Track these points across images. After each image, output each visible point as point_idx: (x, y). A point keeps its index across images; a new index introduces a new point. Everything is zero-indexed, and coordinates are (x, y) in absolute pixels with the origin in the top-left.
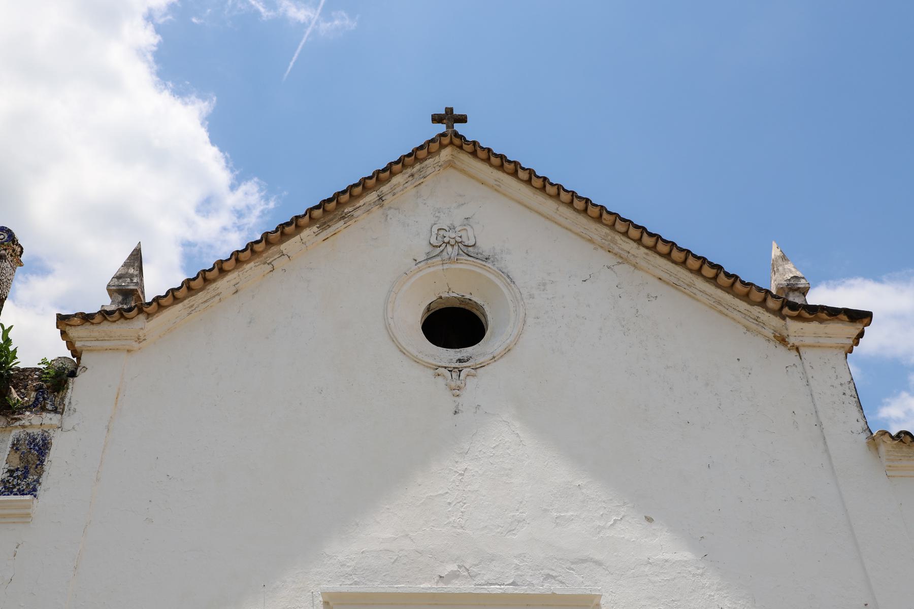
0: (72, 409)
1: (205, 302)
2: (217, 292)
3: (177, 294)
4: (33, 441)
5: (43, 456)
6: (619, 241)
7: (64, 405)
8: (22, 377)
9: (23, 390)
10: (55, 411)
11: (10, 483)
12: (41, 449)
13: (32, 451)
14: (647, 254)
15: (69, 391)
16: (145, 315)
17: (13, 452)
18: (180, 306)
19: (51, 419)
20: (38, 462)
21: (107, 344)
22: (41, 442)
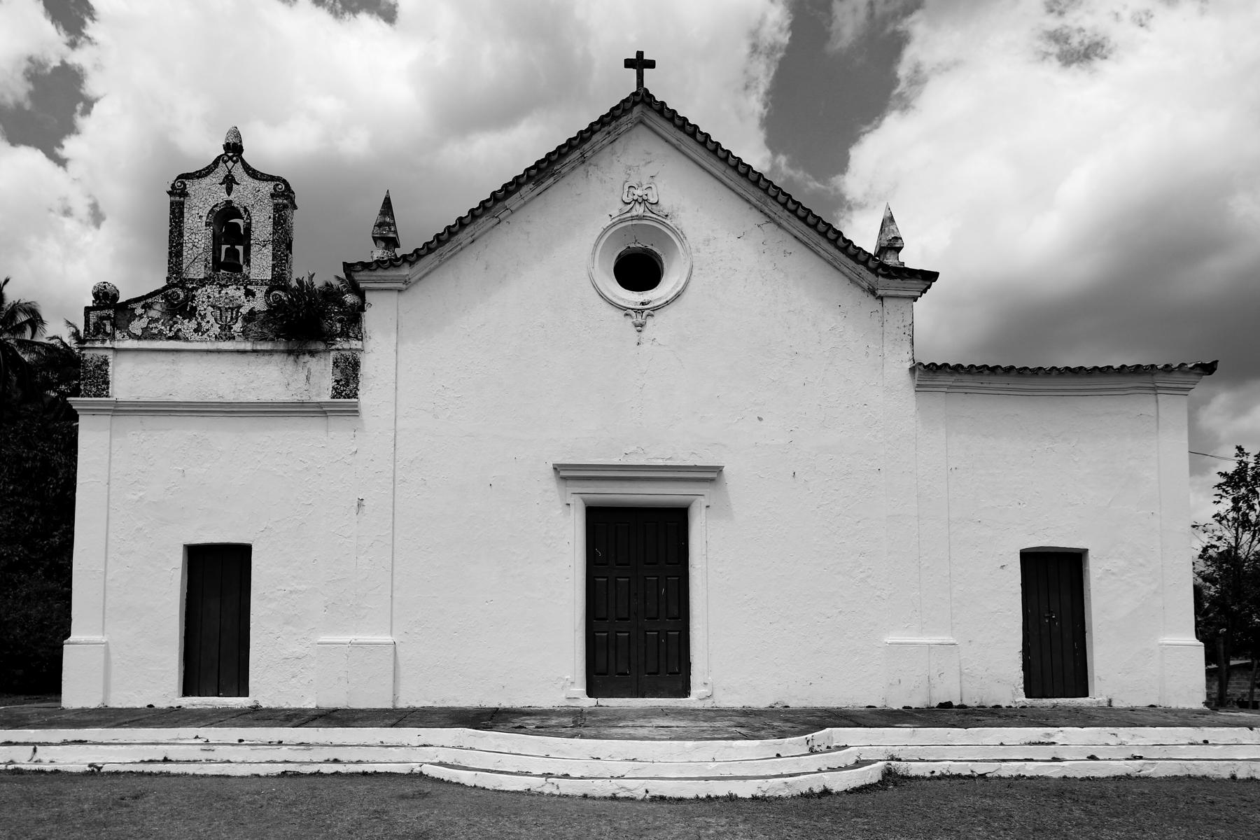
1: (451, 250)
2: (459, 242)
3: (431, 246)
6: (770, 204)
10: (356, 338)
14: (789, 216)
18: (432, 256)
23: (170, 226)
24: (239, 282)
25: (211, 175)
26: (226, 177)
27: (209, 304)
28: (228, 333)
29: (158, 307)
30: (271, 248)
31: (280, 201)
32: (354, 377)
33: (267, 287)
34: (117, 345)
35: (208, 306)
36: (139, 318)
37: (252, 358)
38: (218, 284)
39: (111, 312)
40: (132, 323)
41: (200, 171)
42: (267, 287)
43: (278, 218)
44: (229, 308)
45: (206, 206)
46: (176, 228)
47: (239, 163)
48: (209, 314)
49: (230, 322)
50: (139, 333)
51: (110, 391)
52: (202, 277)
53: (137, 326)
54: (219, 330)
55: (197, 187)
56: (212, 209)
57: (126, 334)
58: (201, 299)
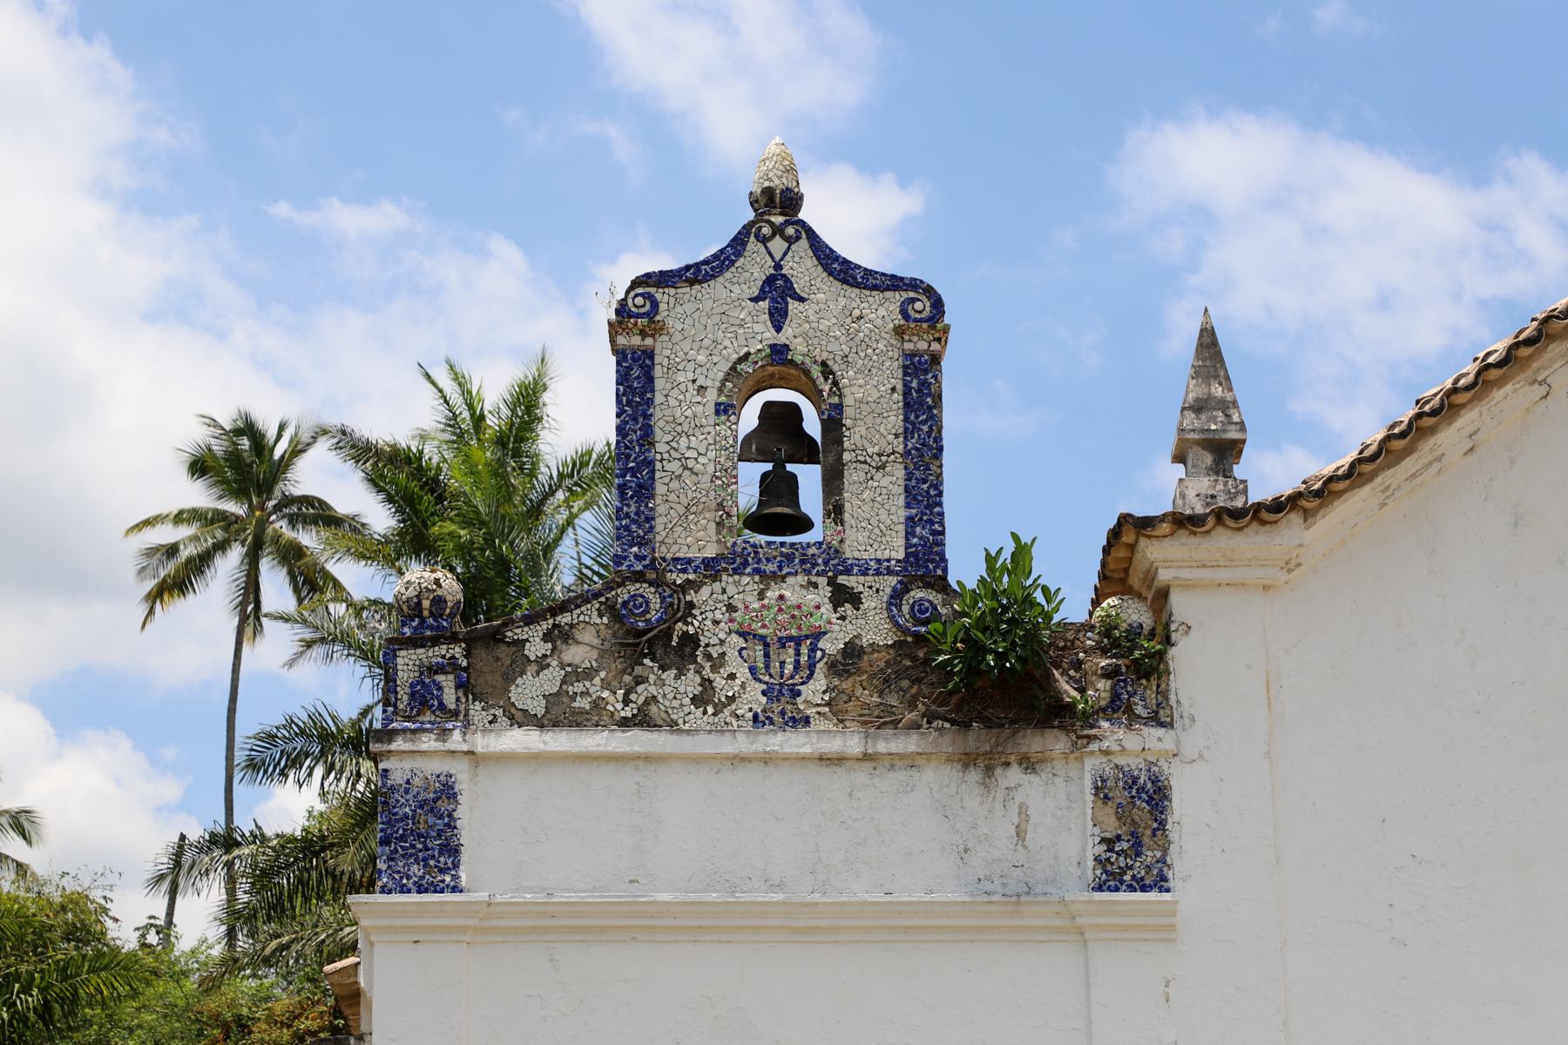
0: (1185, 715)
4: (1134, 782)
5: (1161, 813)
7: (1172, 707)
8: (1062, 644)
9: (1072, 673)
11: (1112, 864)
12: (1154, 799)
13: (1138, 803)
15: (1172, 676)
16: (1301, 513)
17: (1100, 803)
20: (1155, 825)
21: (1224, 575)
22: (1149, 785)
23: (618, 416)
24: (815, 565)
25: (728, 275)
26: (770, 280)
27: (734, 626)
28: (789, 707)
29: (587, 636)
30: (900, 473)
31: (922, 345)
32: (1154, 831)
33: (893, 580)
36: (534, 668)
37: (859, 775)
38: (757, 571)
39: (458, 651)
40: (519, 681)
41: (697, 265)
42: (893, 580)
44: (791, 638)
45: (715, 359)
46: (635, 420)
47: (804, 243)
48: (732, 654)
49: (792, 677)
50: (538, 708)
51: (463, 876)
52: (710, 552)
53: (530, 691)
54: (764, 700)
55: (689, 307)
56: (733, 368)
57: (499, 712)
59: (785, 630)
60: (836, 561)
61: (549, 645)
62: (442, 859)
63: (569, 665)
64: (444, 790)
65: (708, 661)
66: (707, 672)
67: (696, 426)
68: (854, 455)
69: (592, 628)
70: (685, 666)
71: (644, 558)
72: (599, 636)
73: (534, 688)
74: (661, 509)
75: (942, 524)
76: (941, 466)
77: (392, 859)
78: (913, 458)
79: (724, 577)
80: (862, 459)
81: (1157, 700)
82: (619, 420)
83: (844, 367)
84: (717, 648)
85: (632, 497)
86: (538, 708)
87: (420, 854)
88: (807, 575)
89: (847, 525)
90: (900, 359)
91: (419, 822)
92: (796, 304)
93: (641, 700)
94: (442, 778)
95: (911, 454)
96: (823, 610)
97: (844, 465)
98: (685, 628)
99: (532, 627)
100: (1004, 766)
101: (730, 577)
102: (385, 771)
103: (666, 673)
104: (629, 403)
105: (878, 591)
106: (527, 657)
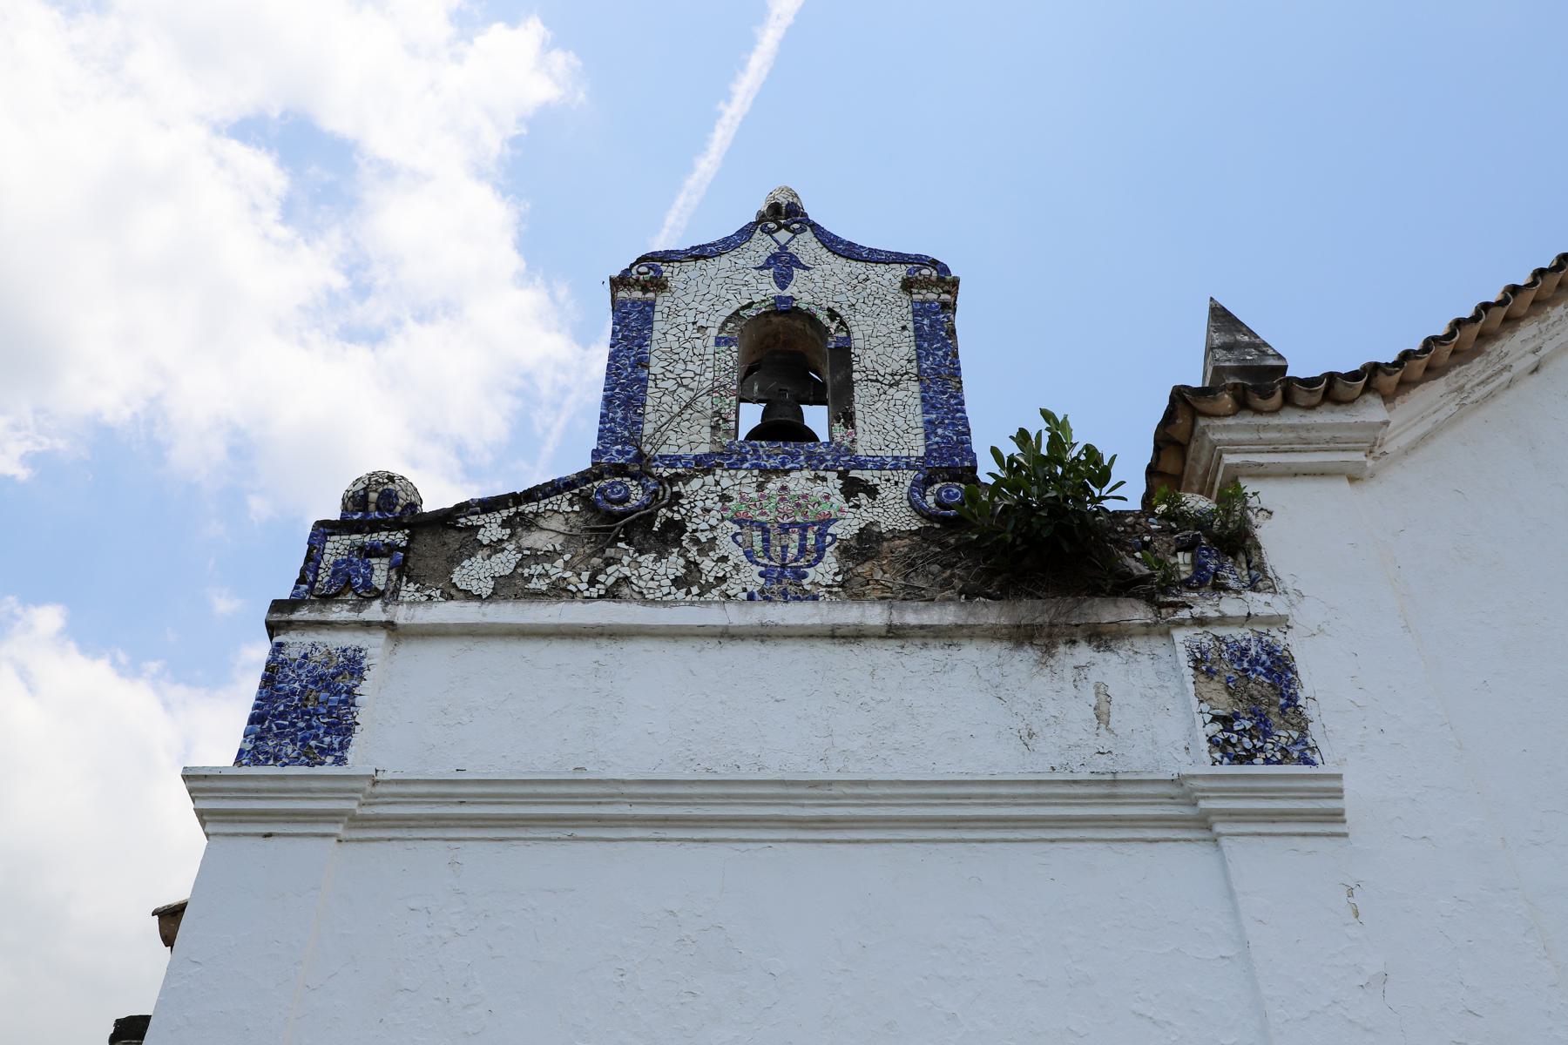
5: (1288, 686)
11: (1234, 745)
12: (1275, 672)
15: (1263, 550)
17: (1202, 678)
18: (1439, 386)
19: (1268, 604)
20: (1282, 701)
22: (1264, 657)
23: (612, 346)
27: (729, 514)
30: (915, 387)
32: (1283, 709)
34: (401, 615)
35: (723, 519)
36: (486, 552)
37: (884, 654)
40: (466, 563)
43: (931, 326)
52: (704, 449)
58: (700, 504)
59: (788, 518)
60: (848, 458)
61: (508, 531)
62: (327, 739)
63: (528, 549)
64: (348, 666)
65: (694, 545)
66: (693, 554)
67: (694, 354)
68: (864, 375)
69: (561, 517)
70: (667, 550)
71: (628, 453)
72: (567, 524)
73: (483, 570)
74: (651, 417)
75: (966, 425)
76: (960, 382)
77: (261, 739)
78: (928, 375)
79: (718, 471)
80: (874, 378)
81: (1250, 577)
82: (612, 349)
83: (852, 312)
84: (707, 533)
85: (619, 406)
86: (484, 589)
87: (299, 733)
88: (813, 470)
89: (859, 430)
90: (910, 307)
91: (307, 699)
92: (801, 271)
93: (611, 580)
94: (349, 653)
95: (926, 372)
96: (832, 499)
97: (854, 382)
98: (669, 514)
99: (489, 515)
100: (1070, 644)
101: (724, 472)
102: (280, 645)
103: (643, 557)
104: (624, 337)
105: (896, 483)
106: (480, 541)
